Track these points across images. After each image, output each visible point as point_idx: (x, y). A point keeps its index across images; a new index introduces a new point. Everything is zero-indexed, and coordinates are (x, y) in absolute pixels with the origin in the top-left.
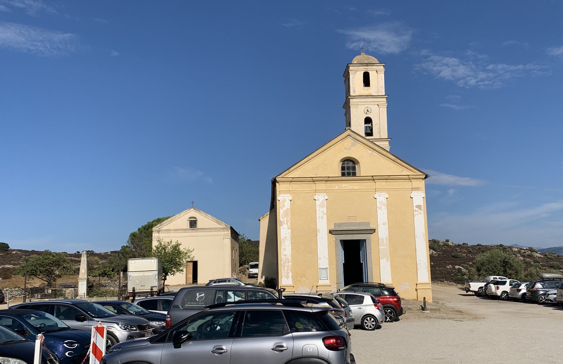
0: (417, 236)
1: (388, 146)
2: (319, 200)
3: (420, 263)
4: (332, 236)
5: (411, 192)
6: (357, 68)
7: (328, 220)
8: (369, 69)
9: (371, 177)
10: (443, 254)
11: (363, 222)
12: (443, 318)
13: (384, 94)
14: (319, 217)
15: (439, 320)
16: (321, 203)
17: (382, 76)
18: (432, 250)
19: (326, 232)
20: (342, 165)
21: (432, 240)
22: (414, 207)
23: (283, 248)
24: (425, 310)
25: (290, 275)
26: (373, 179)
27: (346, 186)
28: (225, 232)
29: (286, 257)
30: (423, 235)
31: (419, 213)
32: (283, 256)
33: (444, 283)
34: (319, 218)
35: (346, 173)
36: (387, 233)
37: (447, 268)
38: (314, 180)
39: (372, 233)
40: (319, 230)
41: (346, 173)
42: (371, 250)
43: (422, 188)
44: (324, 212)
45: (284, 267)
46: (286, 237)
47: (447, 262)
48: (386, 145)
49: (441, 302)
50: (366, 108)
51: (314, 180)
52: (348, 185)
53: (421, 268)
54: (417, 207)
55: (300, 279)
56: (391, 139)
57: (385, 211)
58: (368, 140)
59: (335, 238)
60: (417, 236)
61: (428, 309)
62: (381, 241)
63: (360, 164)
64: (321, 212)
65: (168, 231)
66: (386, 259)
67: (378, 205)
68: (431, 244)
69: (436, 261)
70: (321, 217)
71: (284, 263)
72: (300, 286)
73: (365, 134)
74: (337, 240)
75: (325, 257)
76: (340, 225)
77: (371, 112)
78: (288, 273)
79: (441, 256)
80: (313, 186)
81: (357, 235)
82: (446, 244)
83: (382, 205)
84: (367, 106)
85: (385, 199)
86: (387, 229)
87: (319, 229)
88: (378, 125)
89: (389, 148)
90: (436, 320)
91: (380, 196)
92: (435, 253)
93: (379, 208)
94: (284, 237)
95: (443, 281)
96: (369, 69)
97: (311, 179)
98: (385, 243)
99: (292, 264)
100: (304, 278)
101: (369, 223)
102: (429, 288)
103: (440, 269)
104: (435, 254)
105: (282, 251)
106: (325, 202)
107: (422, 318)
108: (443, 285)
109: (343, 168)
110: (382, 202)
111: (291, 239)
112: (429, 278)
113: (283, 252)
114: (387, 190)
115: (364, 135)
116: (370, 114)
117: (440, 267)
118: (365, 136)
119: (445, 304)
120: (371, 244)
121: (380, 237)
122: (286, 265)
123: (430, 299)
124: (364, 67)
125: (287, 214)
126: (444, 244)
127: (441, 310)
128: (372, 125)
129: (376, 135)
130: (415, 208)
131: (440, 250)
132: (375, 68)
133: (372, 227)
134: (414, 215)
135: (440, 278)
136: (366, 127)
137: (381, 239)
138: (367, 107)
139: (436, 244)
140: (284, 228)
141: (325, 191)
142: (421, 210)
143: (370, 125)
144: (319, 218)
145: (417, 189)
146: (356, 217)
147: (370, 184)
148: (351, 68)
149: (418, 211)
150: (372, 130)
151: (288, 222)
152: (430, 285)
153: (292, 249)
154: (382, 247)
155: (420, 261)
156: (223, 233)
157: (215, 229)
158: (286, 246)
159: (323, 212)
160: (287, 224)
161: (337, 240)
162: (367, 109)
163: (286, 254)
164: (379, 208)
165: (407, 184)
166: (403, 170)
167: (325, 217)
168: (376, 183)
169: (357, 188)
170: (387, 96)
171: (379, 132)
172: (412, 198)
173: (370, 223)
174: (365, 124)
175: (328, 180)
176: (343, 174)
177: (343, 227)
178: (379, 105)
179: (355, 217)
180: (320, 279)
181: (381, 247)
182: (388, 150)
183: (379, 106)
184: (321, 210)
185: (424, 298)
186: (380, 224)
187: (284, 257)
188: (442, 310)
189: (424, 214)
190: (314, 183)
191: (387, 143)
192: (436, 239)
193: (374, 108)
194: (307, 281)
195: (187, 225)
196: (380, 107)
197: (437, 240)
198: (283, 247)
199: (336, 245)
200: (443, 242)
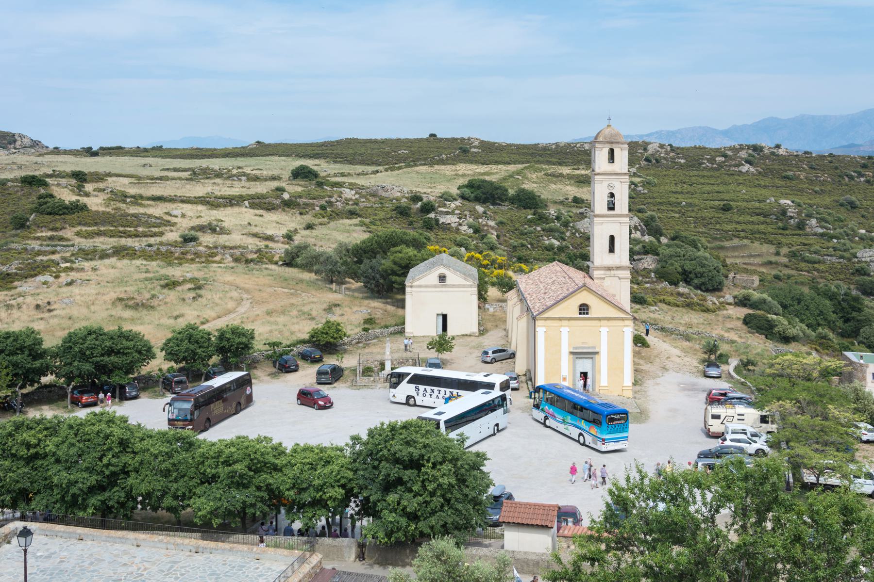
7: (569, 345)
8: (614, 146)
17: (626, 153)
26: (599, 319)
38: (560, 319)
51: (560, 319)
52: (584, 325)
65: (420, 286)
80: (559, 323)
96: (614, 146)
109: (580, 310)
133: (597, 350)
141: (568, 326)
145: (627, 326)
156: (470, 289)
157: (464, 286)
165: (620, 323)
175: (570, 319)
195: (436, 281)
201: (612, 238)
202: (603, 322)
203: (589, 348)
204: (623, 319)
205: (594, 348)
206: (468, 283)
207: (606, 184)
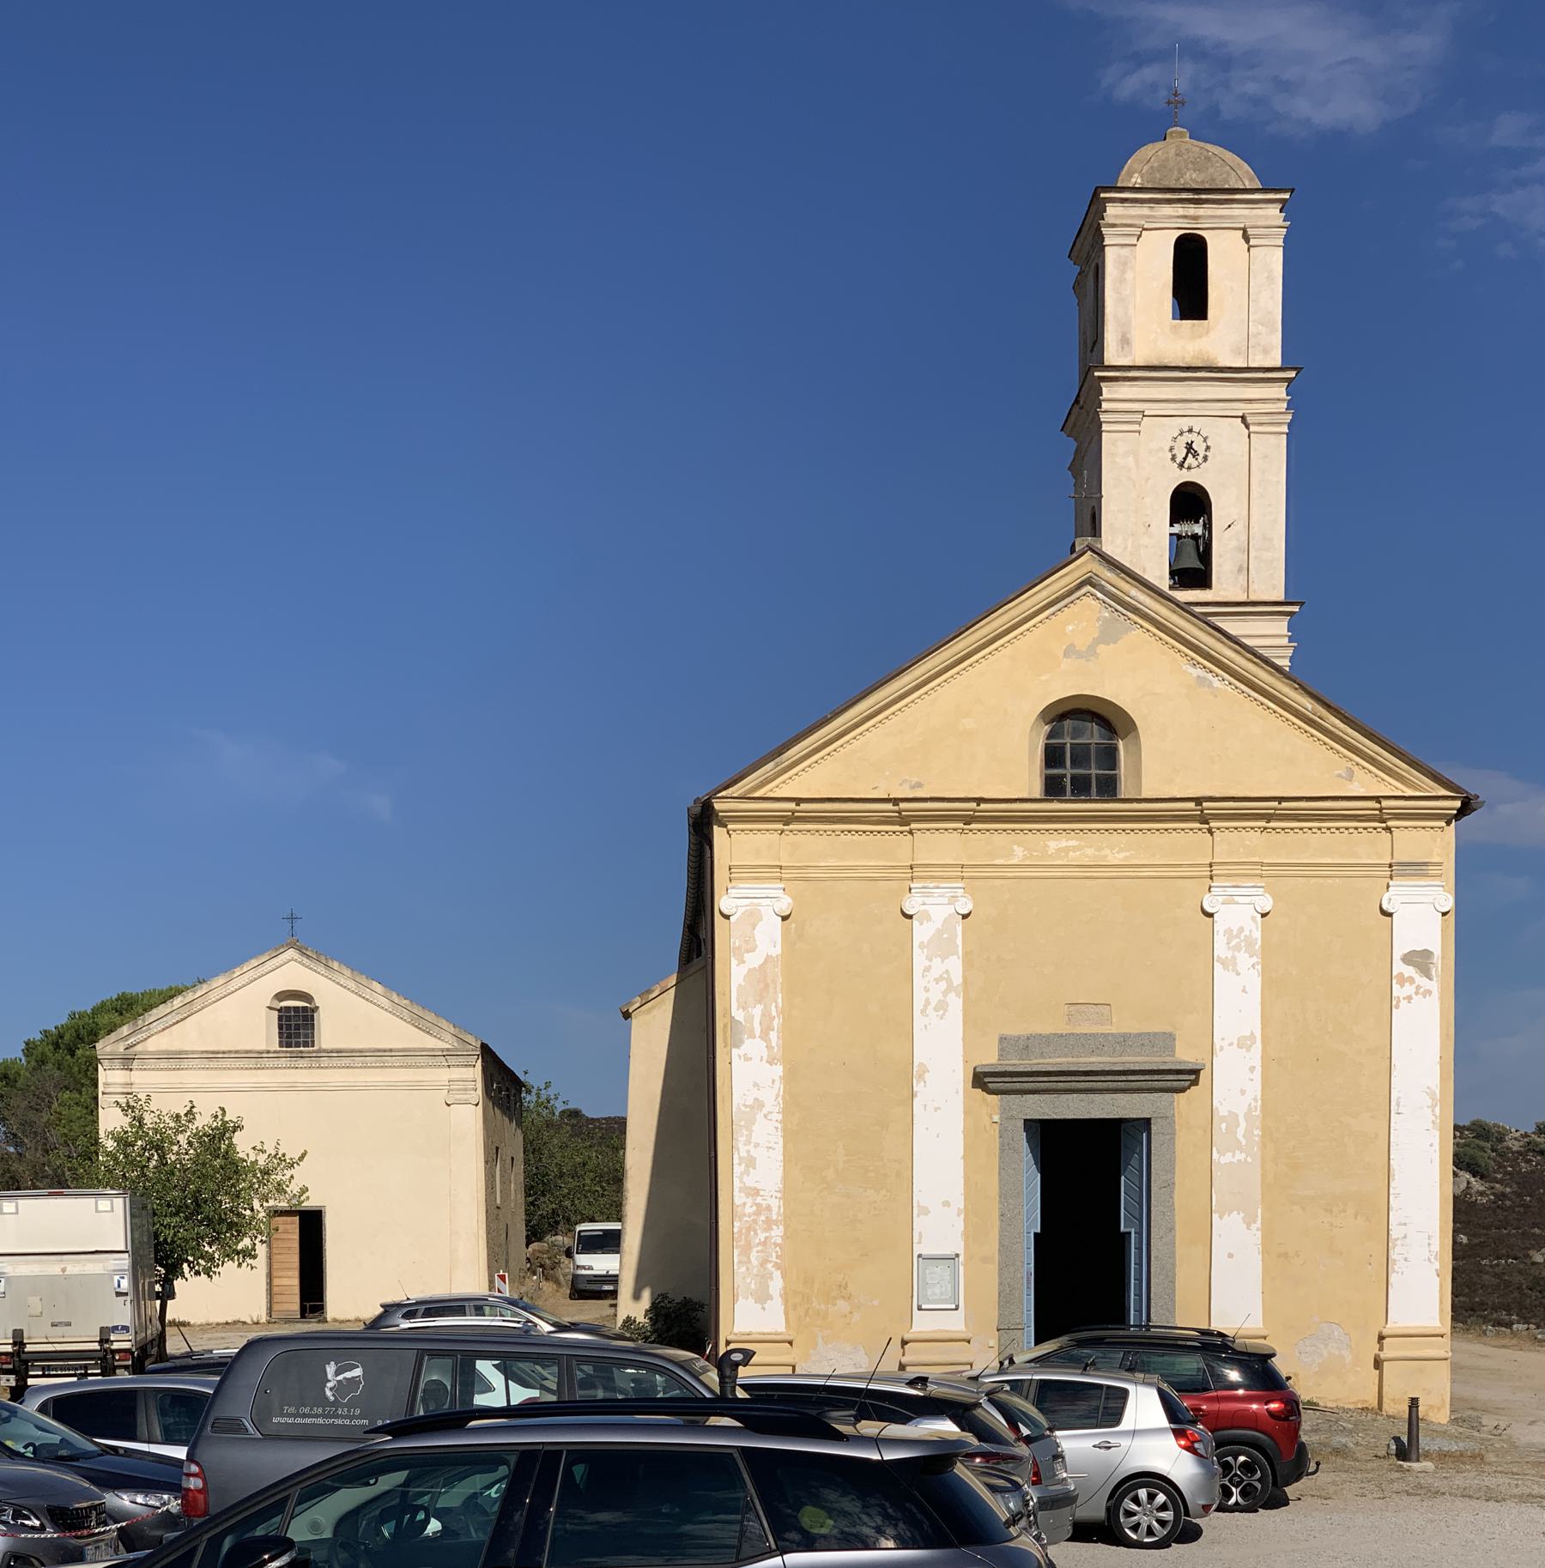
0: (1398, 1104)
1: (1285, 641)
2: (927, 917)
3: (1405, 1237)
4: (984, 1100)
5: (1388, 887)
6: (1144, 210)
7: (969, 1021)
9: (1192, 805)
10: (1519, 1195)
11: (1140, 1035)
12: (1491, 1496)
13: (1278, 363)
14: (927, 1003)
15: (1474, 1503)
16: (939, 932)
17: (1272, 260)
18: (1468, 1176)
19: (959, 1077)
20: (1050, 736)
21: (1474, 1123)
22: (1397, 955)
23: (743, 1154)
24: (1414, 1456)
25: (776, 1284)
27: (1067, 850)
28: (457, 1073)
29: (759, 1200)
30: (1429, 1102)
31: (1417, 994)
32: (742, 1195)
33: (1514, 1334)
34: (923, 1012)
35: (1068, 781)
36: (1255, 1088)
37: (1534, 1264)
39: (1183, 1090)
40: (924, 1069)
41: (1068, 781)
42: (1171, 1170)
43: (1440, 864)
44: (949, 981)
45: (747, 1250)
46: (759, 1104)
47: (1537, 1231)
48: (1271, 634)
49: (1489, 1421)
50: (1181, 434)
53: (1406, 1260)
54: (1408, 959)
55: (823, 1306)
56: (1301, 604)
57: (1254, 981)
58: (1185, 608)
59: (1003, 1111)
60: (1398, 1104)
61: (1427, 1456)
62: (1224, 1126)
63: (1137, 737)
64: (937, 981)
66: (1242, 1215)
67: (1221, 949)
68: (1466, 1145)
69: (1484, 1228)
70: (933, 1004)
71: (749, 1230)
72: (820, 1341)
73: (1172, 574)
74: (1012, 1117)
75: (946, 1204)
77: (1205, 458)
78: (765, 1278)
79: (1508, 1203)
80: (896, 846)
81: (1108, 1097)
82: (1537, 1144)
83: (1237, 948)
85: (1253, 918)
86: (1259, 1070)
87: (921, 1064)
88: (1239, 527)
89: (1290, 652)
90: (1460, 1503)
91: (1230, 900)
92: (1482, 1188)
93: (1223, 963)
94: (750, 1102)
95: (1509, 1325)
97: (889, 806)
98: (1240, 1136)
99: (786, 1237)
100: (841, 1303)
101: (1170, 1037)
102: (1442, 1354)
103: (1497, 1265)
104: (1482, 1194)
105: (738, 1170)
106: (959, 929)
107: (1394, 1496)
108: (1504, 1342)
109: (1053, 756)
110: (1238, 936)
111: (787, 1111)
112: (1441, 1310)
113: (742, 1174)
114: (1266, 871)
115: (1163, 582)
117: (1498, 1258)
118: (1171, 588)
119: (1509, 1430)
120: (1174, 1139)
121: (1221, 1109)
122: (757, 1241)
123: (1439, 1409)
124: (1179, 210)
125: (767, 986)
126: (1529, 1143)
127: (1487, 1460)
128: (1208, 526)
129: (1225, 583)
130: (1399, 967)
131: (1506, 1173)
132: (1240, 213)
133: (1185, 1055)
134: (1394, 1003)
135: (1495, 1309)
136: (1179, 537)
137: (1223, 1119)
138: (1186, 429)
139: (1489, 1145)
140: (747, 1059)
141: (962, 872)
142: (1431, 979)
143: (1198, 529)
144: (923, 1012)
146: (1109, 1005)
147: (1185, 843)
148: (1112, 212)
149: (1411, 980)
150: (1205, 556)
151: (770, 1028)
152: (1447, 1340)
153: (787, 1161)
154: (1227, 1158)
155: (1405, 1224)
158: (757, 1145)
159: (945, 977)
160: (765, 1035)
161: (1012, 1117)
162: (1188, 438)
163: (759, 1186)
164: (1223, 963)
166: (1356, 768)
167: (956, 1004)
168: (1217, 833)
169: (1117, 857)
170: (1292, 374)
171: (1240, 570)
172: (1390, 915)
173: (1174, 1039)
174: (1171, 525)
176: (1053, 788)
177: (1042, 1055)
178: (1249, 419)
179: (1108, 1007)
180: (920, 1309)
181: (1222, 1158)
182: (1284, 663)
183: (1247, 427)
184: (938, 966)
185: (1414, 1403)
186: (1225, 1044)
187: (749, 1201)
188: (1491, 1457)
189: (1442, 999)
190: (907, 828)
191: (1281, 626)
192: (1490, 1119)
193: (1225, 437)
194: (857, 1316)
196: (1252, 428)
197: (1495, 1125)
198: (742, 1150)
199: (1002, 1145)
200: (1526, 1135)
202: (1236, 842)
205: (1167, 1040)
206: (431, 1042)
207: (1160, 436)
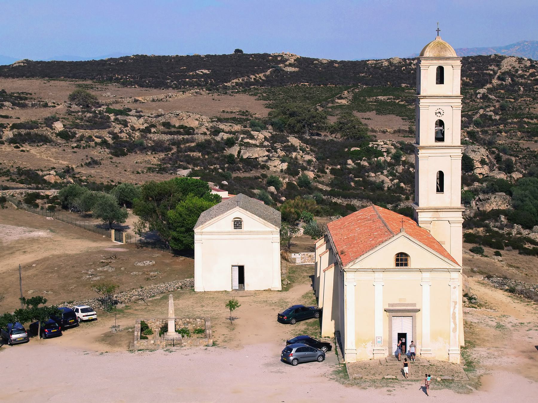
6: (430, 62)
26: (421, 270)
38: (374, 270)
51: (374, 270)
76: (393, 305)
84: (438, 107)
109: (397, 260)
116: (443, 116)
133: (417, 307)
156: (271, 236)
165: (446, 275)
175: (384, 270)
176: (397, 265)
177: (395, 306)
201: (441, 175)
203: (408, 305)
204: (448, 271)
205: (414, 305)
